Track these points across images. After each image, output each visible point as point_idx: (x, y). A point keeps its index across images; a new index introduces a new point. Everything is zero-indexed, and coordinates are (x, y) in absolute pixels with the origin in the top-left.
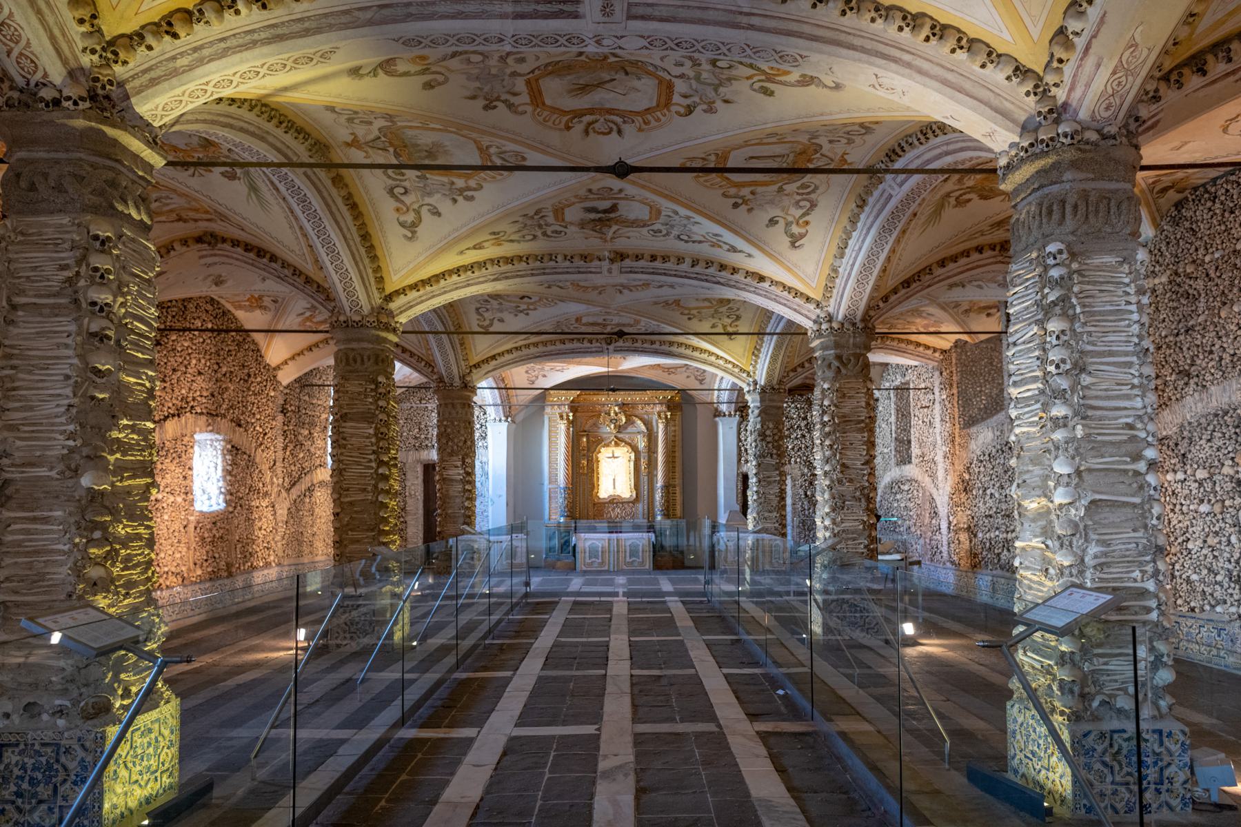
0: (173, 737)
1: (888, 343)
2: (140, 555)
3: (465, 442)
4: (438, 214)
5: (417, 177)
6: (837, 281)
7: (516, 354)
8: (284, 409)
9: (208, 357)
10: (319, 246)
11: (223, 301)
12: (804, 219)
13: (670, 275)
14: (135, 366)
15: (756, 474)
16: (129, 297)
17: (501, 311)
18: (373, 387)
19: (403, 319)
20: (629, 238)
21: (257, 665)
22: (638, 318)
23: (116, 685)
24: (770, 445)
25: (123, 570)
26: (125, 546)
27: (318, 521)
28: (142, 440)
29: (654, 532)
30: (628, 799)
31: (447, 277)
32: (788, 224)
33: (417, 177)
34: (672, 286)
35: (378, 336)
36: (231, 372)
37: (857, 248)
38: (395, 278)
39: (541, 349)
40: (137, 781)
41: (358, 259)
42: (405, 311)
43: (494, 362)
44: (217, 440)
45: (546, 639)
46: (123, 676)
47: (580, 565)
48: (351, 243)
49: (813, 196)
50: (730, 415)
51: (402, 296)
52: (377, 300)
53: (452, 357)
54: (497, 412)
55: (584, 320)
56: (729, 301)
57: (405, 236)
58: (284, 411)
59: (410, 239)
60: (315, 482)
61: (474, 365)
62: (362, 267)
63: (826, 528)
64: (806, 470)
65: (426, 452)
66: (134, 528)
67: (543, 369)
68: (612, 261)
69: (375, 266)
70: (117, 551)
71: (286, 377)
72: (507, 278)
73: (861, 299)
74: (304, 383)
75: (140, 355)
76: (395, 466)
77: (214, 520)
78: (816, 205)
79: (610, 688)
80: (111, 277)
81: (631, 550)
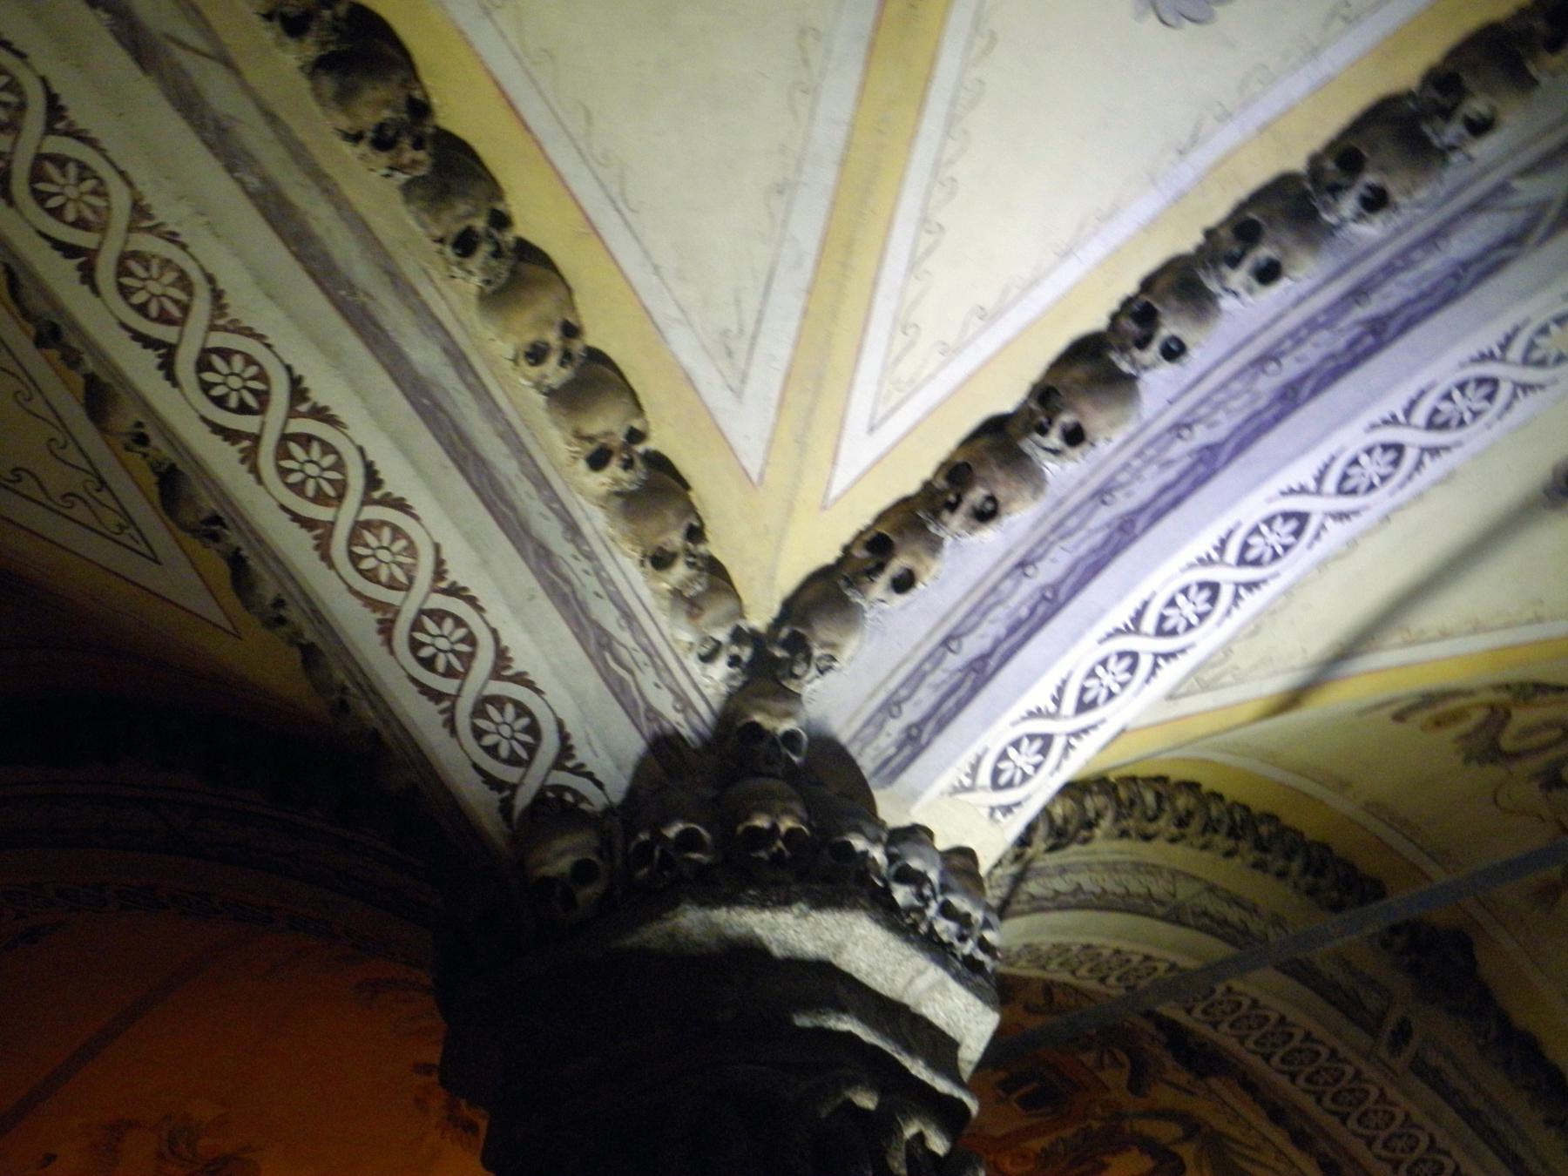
42: (940, 718)
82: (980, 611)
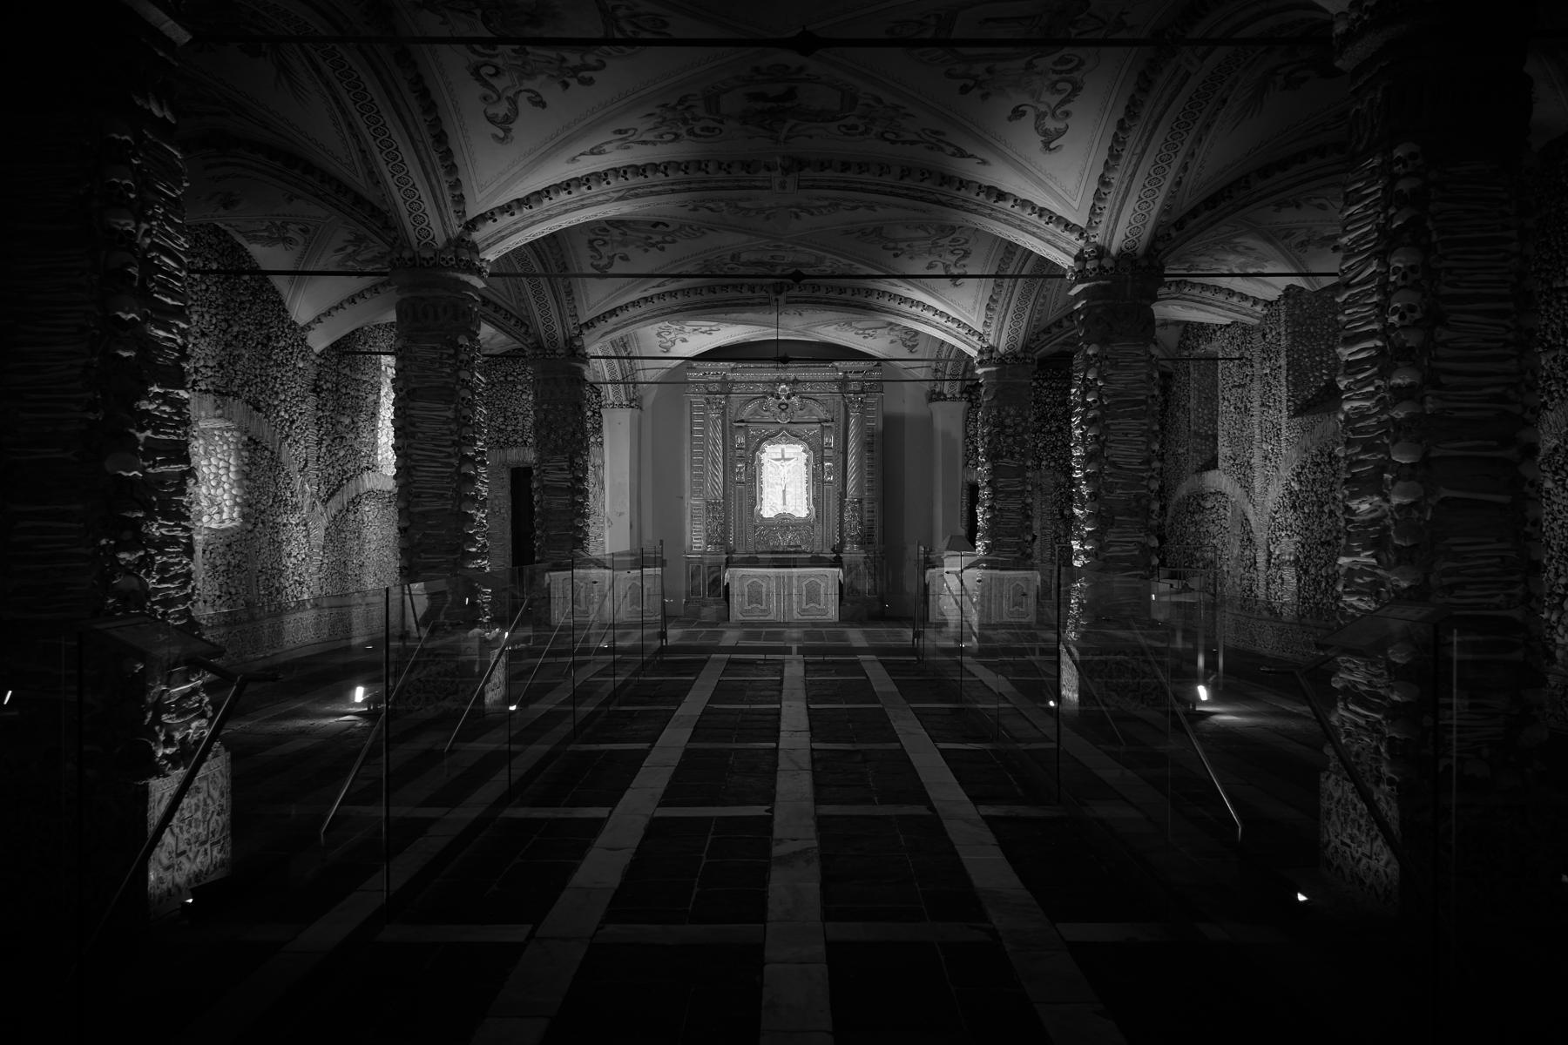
0: (224, 801)
1: (1186, 290)
2: (177, 564)
3: (574, 434)
4: (543, 104)
5: (514, 51)
6: (1109, 197)
7: (644, 308)
8: (317, 386)
9: (213, 311)
10: (376, 150)
11: (231, 231)
12: (1063, 109)
13: (870, 191)
14: (164, 316)
15: (988, 483)
16: (154, 223)
17: (624, 244)
18: (452, 351)
19: (491, 256)
20: (811, 137)
21: (302, 732)
22: (823, 254)
23: (157, 728)
24: (1010, 440)
25: (159, 582)
26: (162, 553)
27: (367, 547)
28: (175, 414)
29: (841, 566)
30: (814, 886)
31: (552, 195)
32: (1040, 116)
33: (514, 51)
34: (871, 207)
35: (457, 280)
36: (245, 333)
37: (1138, 150)
38: (479, 197)
39: (680, 299)
40: (184, 852)
41: (430, 170)
42: (494, 243)
43: (614, 319)
44: (228, 430)
45: (694, 705)
46: (164, 717)
47: (736, 613)
48: (421, 146)
49: (1075, 74)
50: (954, 399)
51: (490, 222)
52: (456, 229)
53: (554, 312)
54: (616, 393)
55: (744, 257)
56: (953, 229)
57: (495, 136)
58: (316, 390)
59: (502, 140)
60: (361, 491)
61: (586, 324)
62: (434, 182)
63: (1085, 553)
64: (1063, 480)
65: (515, 451)
66: (171, 529)
67: (682, 330)
68: (786, 171)
69: (452, 179)
70: (152, 557)
71: (319, 341)
72: (637, 196)
73: (1144, 225)
74: (347, 350)
75: (169, 301)
76: (483, 463)
77: (228, 541)
78: (1081, 88)
79: (783, 763)
80: (132, 196)
81: (808, 592)
82: (506, 228)
